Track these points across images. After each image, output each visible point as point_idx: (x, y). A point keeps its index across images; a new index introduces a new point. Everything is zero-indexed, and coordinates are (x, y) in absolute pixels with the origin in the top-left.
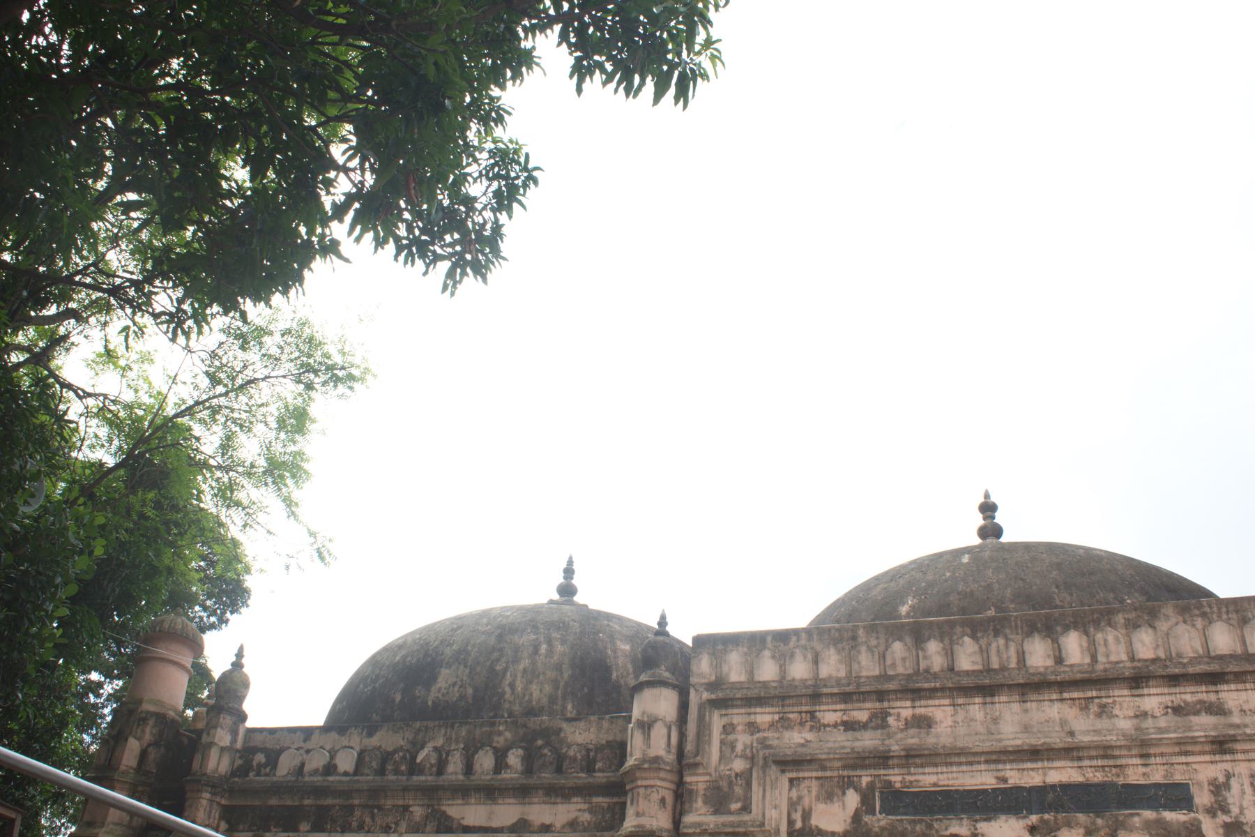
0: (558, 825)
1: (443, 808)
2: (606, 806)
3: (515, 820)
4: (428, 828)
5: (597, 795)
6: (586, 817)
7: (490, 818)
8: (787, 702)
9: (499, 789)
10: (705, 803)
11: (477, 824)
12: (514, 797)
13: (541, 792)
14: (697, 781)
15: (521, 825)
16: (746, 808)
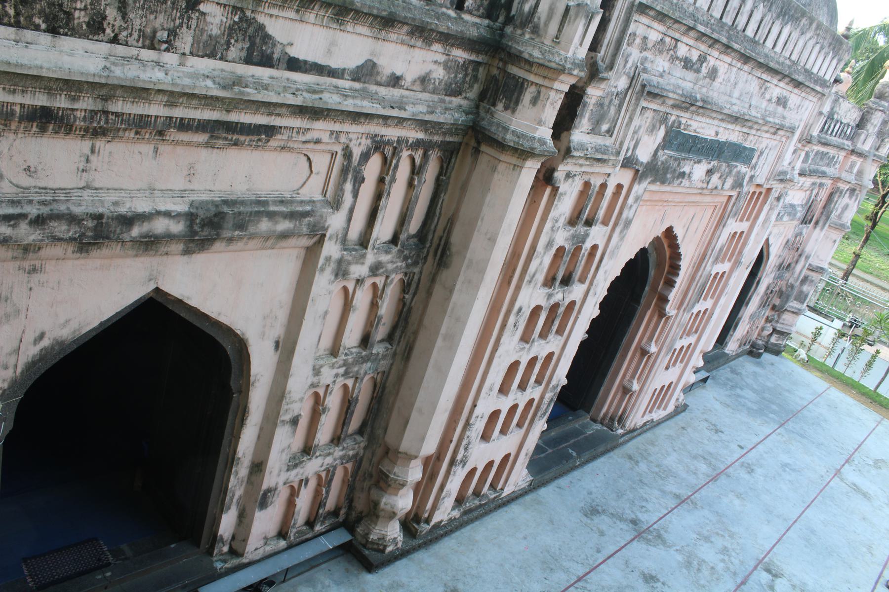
0: (409, 78)
1: (261, 19)
2: (461, 61)
3: (360, 62)
4: (234, 52)
5: (459, 46)
6: (439, 73)
7: (329, 51)
8: (676, 26)
9: (357, 12)
10: (589, 120)
11: (311, 58)
12: (371, 26)
13: (406, 28)
14: (593, 93)
15: (366, 72)
16: (610, 132)
